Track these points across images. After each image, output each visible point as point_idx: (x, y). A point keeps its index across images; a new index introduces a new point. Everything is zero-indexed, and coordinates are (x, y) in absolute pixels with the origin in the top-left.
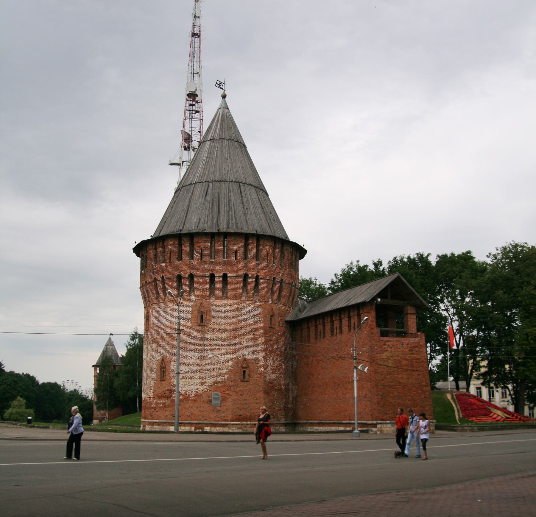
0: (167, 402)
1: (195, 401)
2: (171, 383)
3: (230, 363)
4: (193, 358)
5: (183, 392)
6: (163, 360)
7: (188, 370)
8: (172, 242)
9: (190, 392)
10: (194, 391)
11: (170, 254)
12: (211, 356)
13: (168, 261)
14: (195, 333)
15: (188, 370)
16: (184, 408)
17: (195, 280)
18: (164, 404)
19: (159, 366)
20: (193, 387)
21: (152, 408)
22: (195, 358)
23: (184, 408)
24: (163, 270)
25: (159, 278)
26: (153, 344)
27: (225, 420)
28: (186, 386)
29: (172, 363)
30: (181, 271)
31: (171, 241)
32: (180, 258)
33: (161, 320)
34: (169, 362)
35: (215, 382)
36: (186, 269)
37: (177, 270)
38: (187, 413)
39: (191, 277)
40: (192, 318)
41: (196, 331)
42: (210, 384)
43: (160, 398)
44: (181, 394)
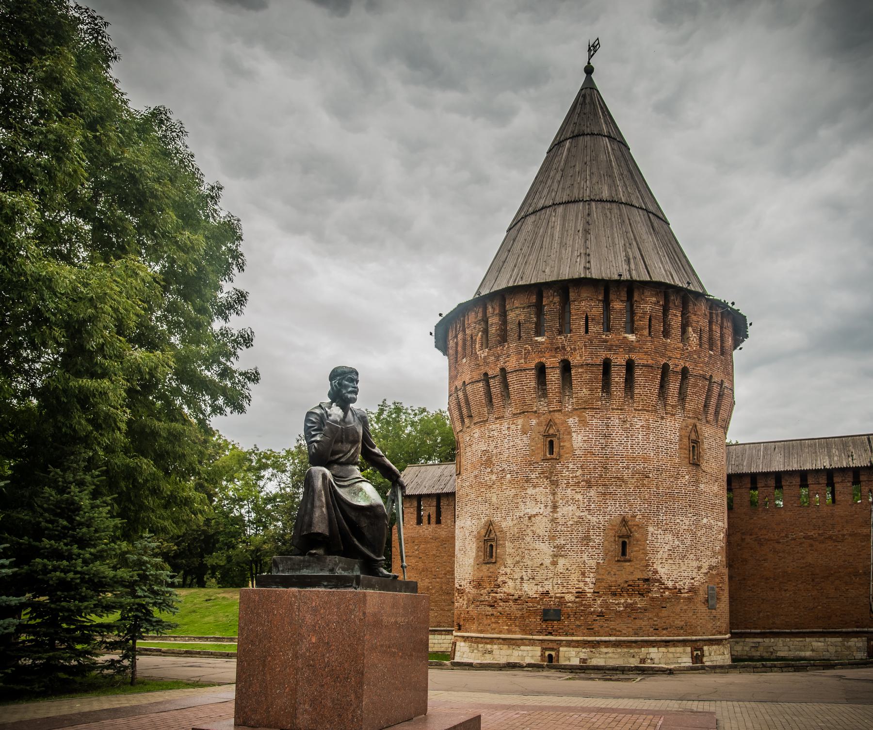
0: (640, 602)
1: (689, 599)
2: (648, 565)
3: (722, 535)
4: (685, 522)
5: (670, 584)
6: (624, 521)
7: (677, 543)
8: (654, 299)
9: (681, 583)
10: (688, 581)
11: (650, 320)
12: (705, 521)
13: (646, 332)
14: (687, 477)
15: (677, 543)
16: (673, 612)
17: (692, 380)
18: (627, 606)
19: (612, 533)
20: (686, 574)
21: (592, 613)
22: (687, 523)
23: (673, 612)
24: (630, 348)
25: (619, 360)
26: (590, 487)
27: (720, 633)
28: (675, 572)
29: (651, 529)
30: (670, 358)
31: (652, 296)
32: (666, 334)
33: (614, 444)
34: (642, 528)
35: (711, 568)
36: (679, 356)
37: (663, 355)
38: (679, 623)
39: (685, 372)
40: (680, 448)
41: (688, 473)
42: (706, 571)
43: (614, 594)
44: (667, 588)
